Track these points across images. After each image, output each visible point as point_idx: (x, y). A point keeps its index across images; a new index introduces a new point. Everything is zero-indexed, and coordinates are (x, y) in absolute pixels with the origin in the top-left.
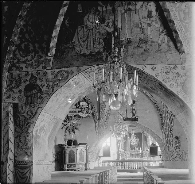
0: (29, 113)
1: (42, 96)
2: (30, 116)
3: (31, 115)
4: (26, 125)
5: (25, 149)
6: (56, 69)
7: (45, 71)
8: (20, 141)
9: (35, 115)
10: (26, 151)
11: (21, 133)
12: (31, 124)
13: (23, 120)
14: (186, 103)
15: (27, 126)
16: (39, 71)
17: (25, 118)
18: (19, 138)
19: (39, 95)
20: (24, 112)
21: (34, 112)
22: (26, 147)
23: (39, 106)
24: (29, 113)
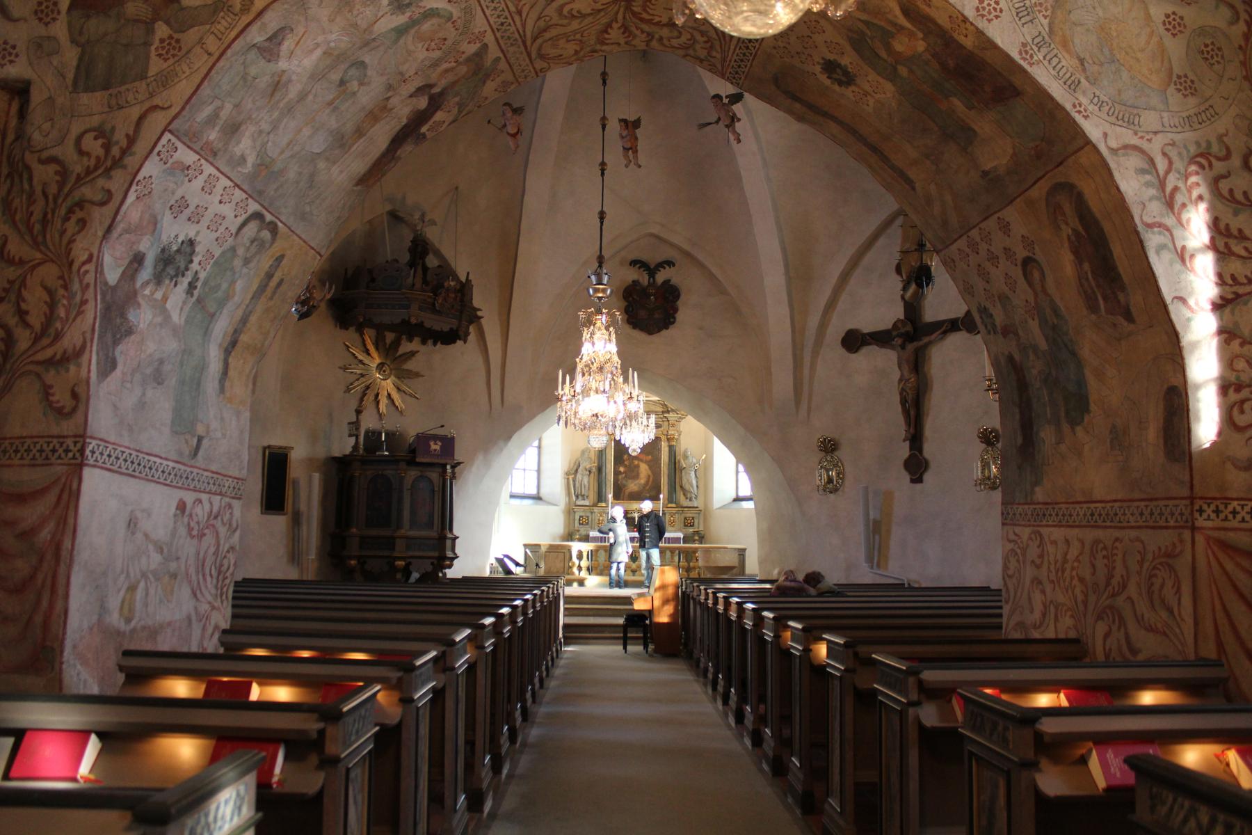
1: (178, 41)
2: (93, 162)
3: (101, 152)
4: (67, 219)
5: (50, 363)
8: (22, 314)
9: (124, 152)
10: (50, 377)
11: (34, 267)
13: (53, 189)
14: (1079, 118)
15: (71, 226)
17: (64, 173)
18: (19, 295)
19: (162, 30)
20: (62, 141)
21: (120, 137)
22: (49, 353)
23: (157, 101)
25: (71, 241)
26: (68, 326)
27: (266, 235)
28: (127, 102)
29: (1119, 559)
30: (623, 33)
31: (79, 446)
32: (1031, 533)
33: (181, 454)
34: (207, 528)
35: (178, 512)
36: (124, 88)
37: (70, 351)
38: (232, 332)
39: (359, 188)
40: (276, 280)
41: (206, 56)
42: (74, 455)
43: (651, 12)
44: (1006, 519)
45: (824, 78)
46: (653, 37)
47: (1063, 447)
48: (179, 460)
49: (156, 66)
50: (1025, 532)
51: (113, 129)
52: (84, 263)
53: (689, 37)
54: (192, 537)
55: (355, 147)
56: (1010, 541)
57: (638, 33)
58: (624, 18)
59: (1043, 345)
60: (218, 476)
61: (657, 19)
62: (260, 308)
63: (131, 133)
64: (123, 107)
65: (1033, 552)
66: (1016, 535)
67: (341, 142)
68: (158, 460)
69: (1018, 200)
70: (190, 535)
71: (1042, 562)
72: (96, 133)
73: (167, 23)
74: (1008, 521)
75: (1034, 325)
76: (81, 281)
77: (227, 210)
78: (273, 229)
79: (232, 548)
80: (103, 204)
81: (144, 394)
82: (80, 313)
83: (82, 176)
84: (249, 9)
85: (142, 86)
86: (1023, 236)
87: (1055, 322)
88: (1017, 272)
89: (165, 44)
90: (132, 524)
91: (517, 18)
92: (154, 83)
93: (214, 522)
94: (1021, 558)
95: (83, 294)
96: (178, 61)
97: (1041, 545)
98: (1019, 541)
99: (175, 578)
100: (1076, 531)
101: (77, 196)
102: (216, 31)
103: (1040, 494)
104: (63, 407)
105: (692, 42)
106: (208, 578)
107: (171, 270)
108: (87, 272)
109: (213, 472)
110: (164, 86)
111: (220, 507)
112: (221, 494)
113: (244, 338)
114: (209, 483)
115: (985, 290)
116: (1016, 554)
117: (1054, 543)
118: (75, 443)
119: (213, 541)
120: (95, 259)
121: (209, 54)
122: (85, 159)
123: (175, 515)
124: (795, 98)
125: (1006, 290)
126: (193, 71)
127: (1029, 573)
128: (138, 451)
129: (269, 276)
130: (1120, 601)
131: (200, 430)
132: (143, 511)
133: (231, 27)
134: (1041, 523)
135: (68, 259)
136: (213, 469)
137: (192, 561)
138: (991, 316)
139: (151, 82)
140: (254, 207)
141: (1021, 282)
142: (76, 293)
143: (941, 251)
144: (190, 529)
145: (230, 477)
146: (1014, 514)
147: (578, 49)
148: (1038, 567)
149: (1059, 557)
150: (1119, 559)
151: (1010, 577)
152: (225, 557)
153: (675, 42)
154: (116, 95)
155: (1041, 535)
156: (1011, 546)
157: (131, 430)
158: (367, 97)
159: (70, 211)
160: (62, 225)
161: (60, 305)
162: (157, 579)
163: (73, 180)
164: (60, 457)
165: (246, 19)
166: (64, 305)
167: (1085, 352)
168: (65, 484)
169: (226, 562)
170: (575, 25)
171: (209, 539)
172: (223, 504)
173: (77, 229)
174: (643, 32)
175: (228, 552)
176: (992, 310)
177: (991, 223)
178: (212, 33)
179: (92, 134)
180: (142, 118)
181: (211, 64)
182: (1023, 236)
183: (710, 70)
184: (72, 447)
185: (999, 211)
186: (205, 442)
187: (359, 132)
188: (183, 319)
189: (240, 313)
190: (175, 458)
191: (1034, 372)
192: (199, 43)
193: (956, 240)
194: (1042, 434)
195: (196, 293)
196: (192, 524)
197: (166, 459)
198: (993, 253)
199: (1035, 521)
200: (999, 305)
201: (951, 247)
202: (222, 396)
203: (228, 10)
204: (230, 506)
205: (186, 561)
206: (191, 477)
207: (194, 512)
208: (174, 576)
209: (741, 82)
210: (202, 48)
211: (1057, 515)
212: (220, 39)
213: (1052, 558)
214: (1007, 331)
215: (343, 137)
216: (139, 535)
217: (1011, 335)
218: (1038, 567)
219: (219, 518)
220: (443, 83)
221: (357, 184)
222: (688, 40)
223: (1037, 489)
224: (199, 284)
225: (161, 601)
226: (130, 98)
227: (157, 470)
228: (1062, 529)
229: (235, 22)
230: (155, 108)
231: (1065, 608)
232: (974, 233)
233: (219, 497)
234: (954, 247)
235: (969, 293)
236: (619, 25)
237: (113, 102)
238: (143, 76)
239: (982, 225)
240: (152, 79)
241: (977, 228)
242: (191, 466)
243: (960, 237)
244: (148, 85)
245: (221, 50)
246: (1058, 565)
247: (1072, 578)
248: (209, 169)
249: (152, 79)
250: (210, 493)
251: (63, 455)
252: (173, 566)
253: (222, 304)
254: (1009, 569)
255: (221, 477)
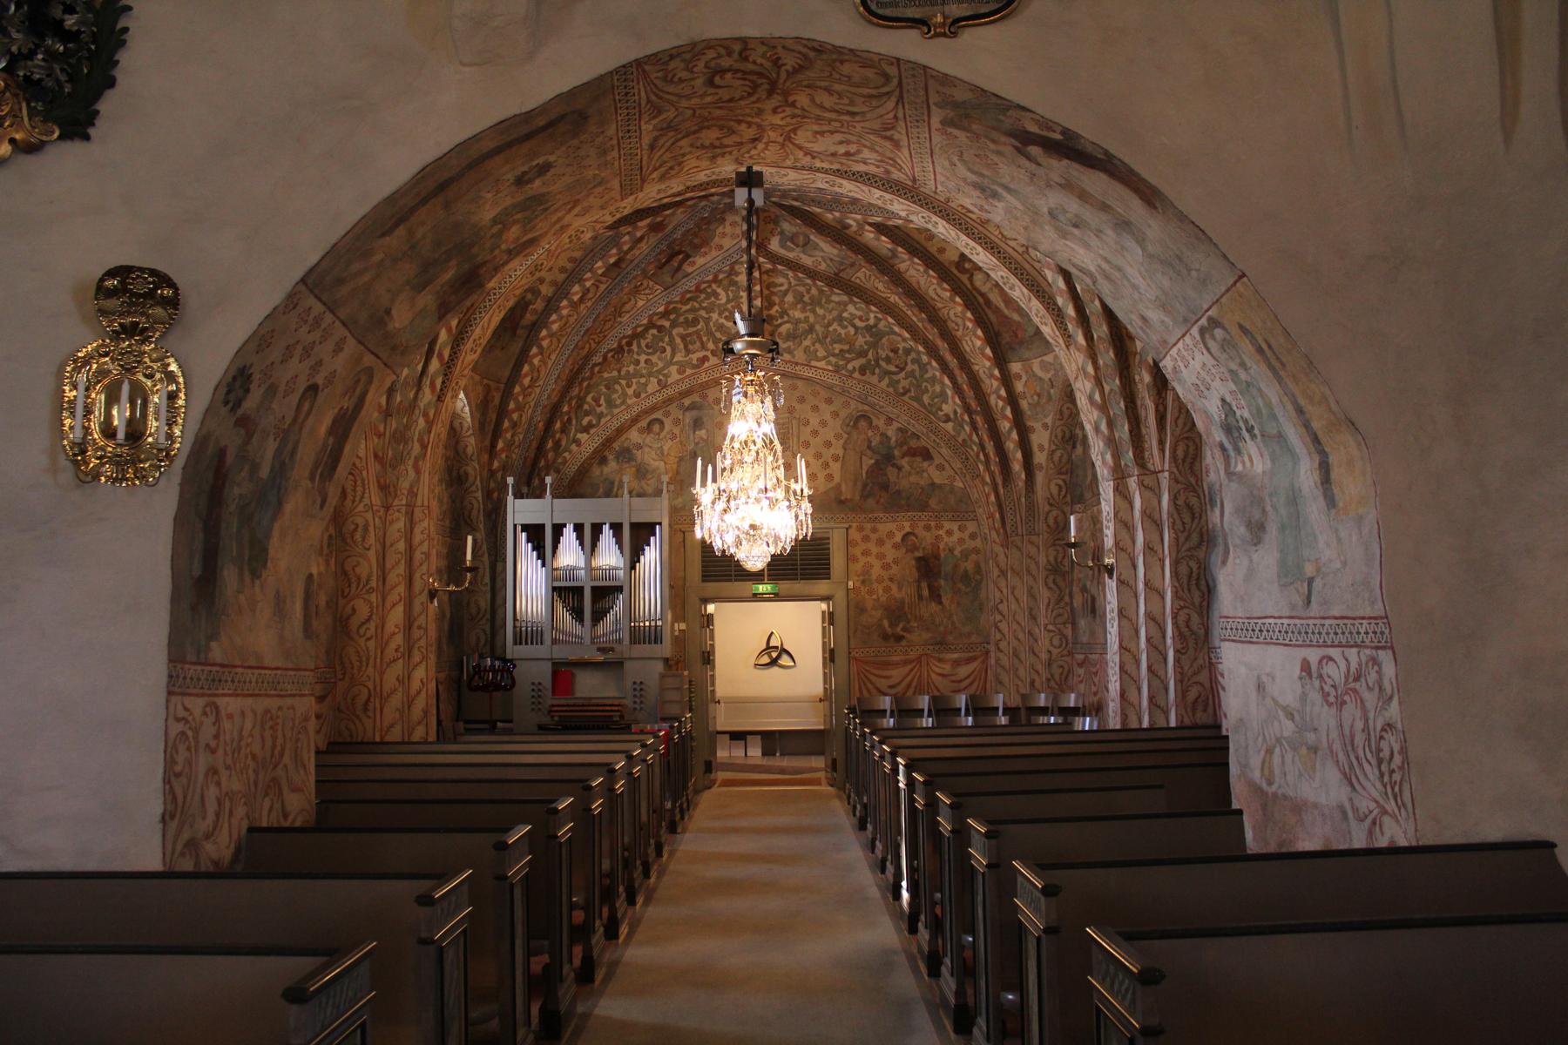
27: (1218, 333)
29: (280, 728)
30: (779, 58)
32: (206, 706)
33: (1293, 607)
34: (1346, 693)
35: (1304, 674)
38: (1304, 430)
39: (1158, 205)
40: (1264, 346)
43: (747, 83)
44: (174, 685)
45: (541, 160)
46: (740, 54)
47: (242, 597)
48: (1293, 614)
50: (196, 705)
53: (695, 69)
54: (1330, 705)
55: (1119, 210)
56: (178, 720)
57: (759, 61)
58: (778, 74)
59: (265, 472)
60: (1346, 621)
61: (739, 75)
62: (1291, 385)
65: (208, 730)
66: (186, 709)
67: (1123, 225)
68: (1271, 621)
69: (362, 348)
70: (1327, 702)
71: (218, 746)
74: (176, 690)
75: (271, 446)
77: (1198, 357)
78: (1214, 323)
79: (1388, 727)
81: (1251, 561)
86: (335, 371)
87: (287, 461)
88: (302, 386)
90: (1260, 687)
91: (900, 115)
93: (1357, 686)
94: (193, 744)
97: (217, 721)
98: (190, 718)
99: (1316, 753)
100: (250, 701)
103: (217, 652)
105: (691, 66)
106: (1366, 765)
107: (1236, 434)
109: (1336, 618)
111: (1360, 664)
112: (1356, 645)
113: (1315, 425)
114: (1336, 634)
115: (273, 363)
116: (187, 738)
117: (230, 716)
119: (1358, 714)
123: (1301, 678)
124: (551, 124)
125: (282, 388)
127: (203, 762)
128: (1248, 618)
129: (1260, 351)
130: (280, 772)
131: (1309, 570)
132: (1268, 675)
134: (217, 692)
136: (1336, 613)
137: (1334, 735)
138: (248, 391)
140: (1195, 331)
141: (295, 398)
143: (306, 285)
144: (1325, 695)
145: (1363, 618)
146: (185, 678)
147: (838, 64)
148: (213, 751)
149: (235, 734)
150: (280, 728)
151: (178, 775)
152: (1381, 738)
153: (711, 54)
155: (217, 708)
156: (180, 727)
157: (1242, 600)
158: (1073, 206)
162: (1294, 749)
167: (288, 507)
169: (1384, 744)
170: (837, 87)
171: (1351, 710)
172: (1364, 659)
174: (754, 63)
175: (1383, 729)
176: (253, 386)
177: (341, 331)
182: (335, 371)
183: (655, 55)
185: (353, 335)
186: (1317, 584)
187: (1105, 208)
188: (1269, 462)
189: (1290, 407)
190: (1287, 614)
191: (237, 491)
193: (320, 299)
194: (225, 573)
195: (1256, 431)
196: (1327, 688)
197: (1280, 618)
198: (312, 349)
199: (209, 689)
200: (262, 390)
201: (312, 296)
202: (1333, 512)
204: (1374, 661)
205: (1328, 735)
206: (1324, 632)
207: (1324, 672)
208: (1314, 750)
209: (616, 78)
211: (233, 681)
213: (228, 737)
214: (244, 423)
215: (1116, 224)
216: (1268, 701)
217: (243, 432)
218: (213, 751)
219: (1363, 680)
220: (1003, 139)
221: (1155, 208)
222: (696, 66)
223: (213, 644)
224: (1252, 422)
225: (1301, 775)
227: (1274, 631)
228: (239, 699)
231: (240, 795)
232: (329, 318)
233: (1354, 650)
234: (312, 301)
235: (259, 345)
236: (783, 68)
239: (338, 323)
241: (334, 319)
242: (1307, 618)
243: (324, 304)
246: (235, 744)
247: (246, 757)
248: (1174, 351)
250: (1339, 646)
252: (1311, 737)
253: (1274, 417)
254: (176, 763)
255: (1349, 622)
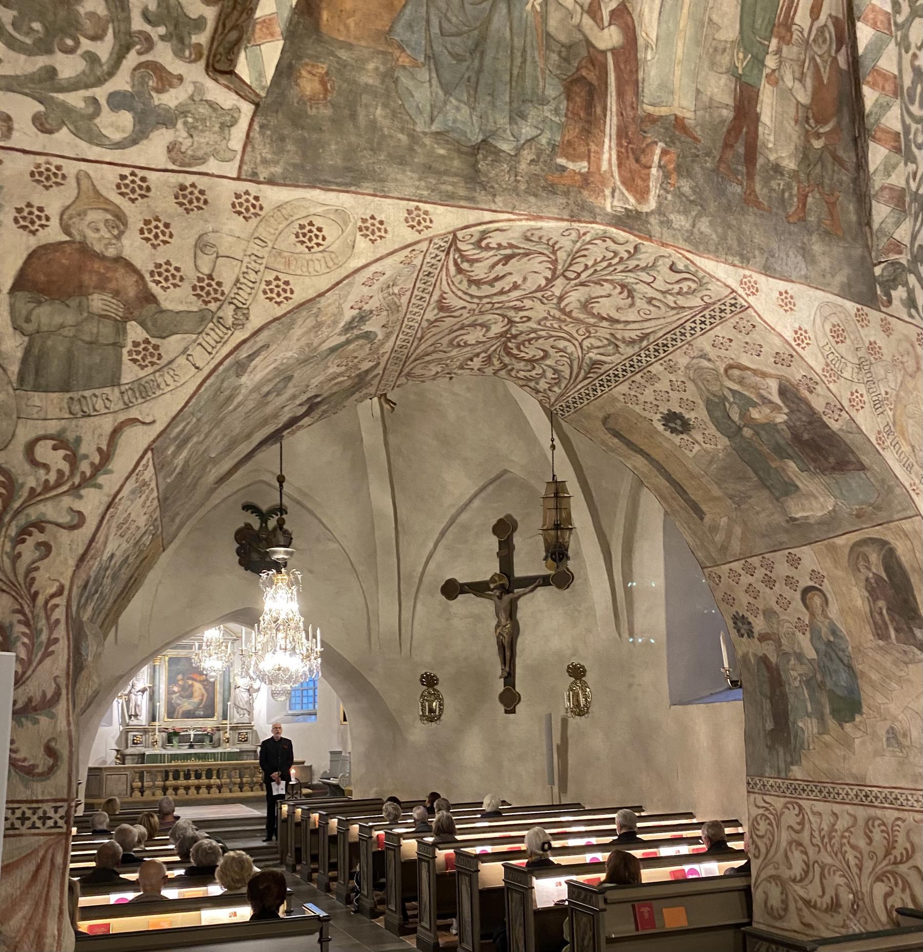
0: (44, 452)
1: (156, 347)
2: (52, 477)
3: (65, 467)
6: (271, 182)
7: (189, 180)
9: (97, 469)
12: (65, 536)
15: (28, 551)
16: (141, 173)
19: (135, 332)
21: (88, 448)
23: (133, 413)
24: (44, 452)
25: (30, 570)
26: (31, 669)
28: (95, 410)
31: (62, 812)
36: (87, 393)
37: (38, 698)
41: (194, 370)
42: (56, 823)
49: (130, 373)
51: (78, 440)
52: (53, 596)
63: (104, 447)
64: (89, 416)
72: (54, 442)
73: (143, 324)
76: (48, 618)
80: (72, 528)
82: (47, 654)
83: (39, 490)
84: (243, 325)
85: (114, 393)
89: (140, 349)
92: (130, 392)
95: (51, 633)
96: (158, 371)
101: (33, 513)
102: (204, 344)
104: (34, 766)
108: (57, 606)
110: (143, 398)
118: (56, 809)
120: (66, 593)
121: (197, 368)
122: (42, 472)
126: (178, 384)
133: (221, 341)
135: (29, 591)
139: (127, 390)
142: (41, 630)
154: (79, 400)
159: (24, 532)
160: (13, 548)
161: (19, 644)
163: (25, 493)
164: (33, 826)
165: (240, 336)
166: (24, 644)
168: (43, 859)
173: (38, 554)
178: (200, 344)
179: (51, 443)
180: (116, 432)
181: (200, 380)
184: (51, 813)
192: (183, 353)
203: (219, 322)
210: (187, 359)
212: (210, 353)
226: (99, 405)
229: (226, 337)
230: (134, 421)
237: (76, 408)
238: (114, 381)
240: (127, 387)
244: (122, 393)
245: (212, 366)
249: (127, 387)
251: (39, 824)
